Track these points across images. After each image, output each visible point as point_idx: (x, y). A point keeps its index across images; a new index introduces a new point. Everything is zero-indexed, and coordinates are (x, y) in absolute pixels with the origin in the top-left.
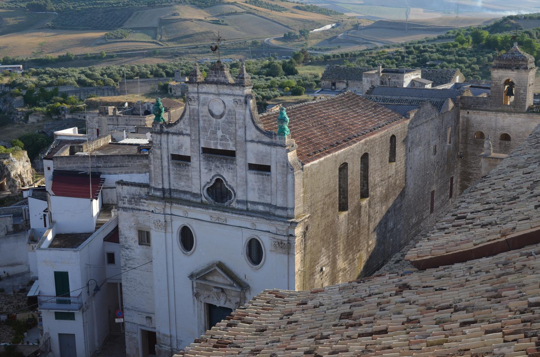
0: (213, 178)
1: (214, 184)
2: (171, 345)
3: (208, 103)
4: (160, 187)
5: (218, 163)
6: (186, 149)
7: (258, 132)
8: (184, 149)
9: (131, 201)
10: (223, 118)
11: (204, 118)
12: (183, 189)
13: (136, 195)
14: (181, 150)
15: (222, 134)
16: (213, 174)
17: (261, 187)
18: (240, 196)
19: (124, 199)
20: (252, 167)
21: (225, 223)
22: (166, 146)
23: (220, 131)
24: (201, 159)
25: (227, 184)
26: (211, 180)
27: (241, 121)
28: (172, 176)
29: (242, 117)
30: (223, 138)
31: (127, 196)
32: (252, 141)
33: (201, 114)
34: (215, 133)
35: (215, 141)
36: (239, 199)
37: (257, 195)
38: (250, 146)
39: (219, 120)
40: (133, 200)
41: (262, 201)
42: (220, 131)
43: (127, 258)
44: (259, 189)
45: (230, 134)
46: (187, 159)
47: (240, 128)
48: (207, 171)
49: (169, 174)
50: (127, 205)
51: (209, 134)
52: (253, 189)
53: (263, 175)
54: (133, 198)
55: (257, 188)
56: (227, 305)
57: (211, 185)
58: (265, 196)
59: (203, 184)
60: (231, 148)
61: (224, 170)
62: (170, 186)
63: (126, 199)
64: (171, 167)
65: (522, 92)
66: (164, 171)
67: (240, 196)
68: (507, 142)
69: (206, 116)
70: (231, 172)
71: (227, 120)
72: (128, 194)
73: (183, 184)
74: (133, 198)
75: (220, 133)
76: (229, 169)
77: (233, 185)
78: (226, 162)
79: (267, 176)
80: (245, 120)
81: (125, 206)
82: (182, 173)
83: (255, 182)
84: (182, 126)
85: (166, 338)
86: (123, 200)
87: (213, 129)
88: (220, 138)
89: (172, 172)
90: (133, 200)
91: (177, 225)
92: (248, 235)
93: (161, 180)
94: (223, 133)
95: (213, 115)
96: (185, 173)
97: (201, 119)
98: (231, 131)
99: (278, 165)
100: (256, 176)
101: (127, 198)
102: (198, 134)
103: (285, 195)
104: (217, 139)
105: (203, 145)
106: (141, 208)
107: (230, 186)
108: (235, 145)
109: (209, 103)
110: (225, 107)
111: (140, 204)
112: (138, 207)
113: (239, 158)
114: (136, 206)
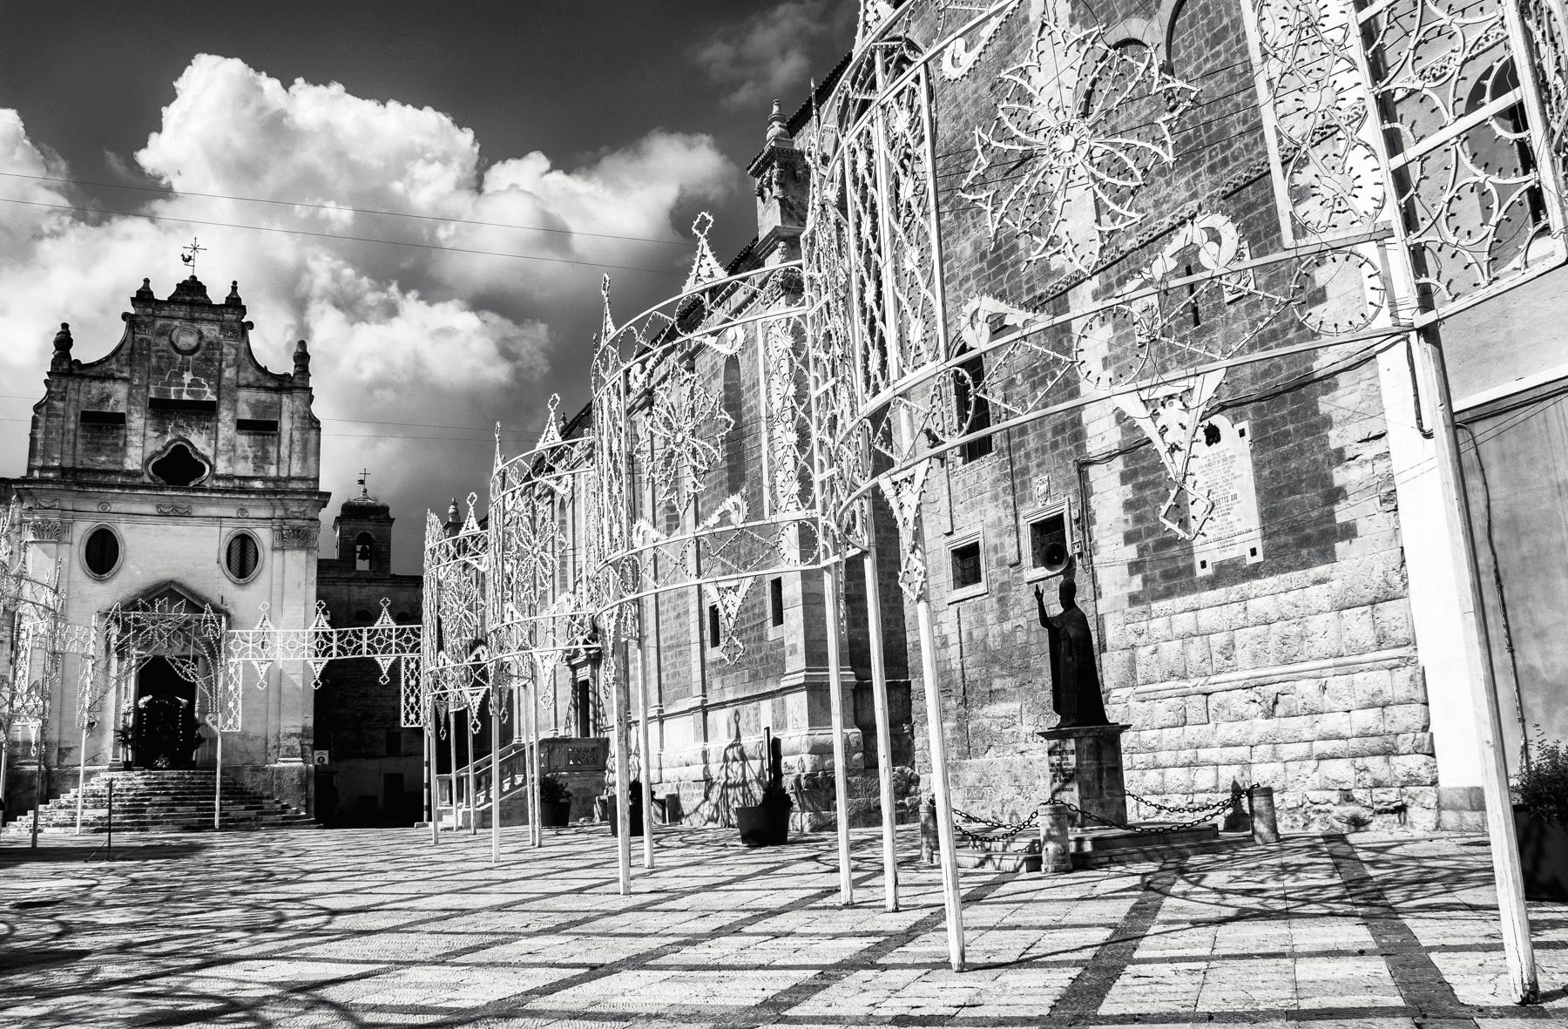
0: (170, 443)
4: (56, 464)
5: (181, 422)
8: (112, 401)
10: (197, 355)
12: (103, 467)
17: (259, 453)
18: (222, 467)
20: (242, 425)
25: (197, 453)
26: (165, 448)
28: (80, 447)
30: (194, 383)
32: (248, 386)
33: (154, 349)
34: (180, 375)
38: (243, 394)
41: (261, 474)
44: (256, 457)
45: (208, 377)
47: (228, 366)
48: (157, 434)
49: (75, 443)
52: (245, 458)
55: (251, 455)
57: (165, 455)
59: (147, 455)
60: (209, 396)
64: (79, 433)
65: (384, 549)
67: (222, 467)
73: (103, 459)
77: (209, 452)
82: (104, 441)
84: (114, 367)
89: (80, 441)
91: (82, 530)
92: (229, 530)
95: (178, 350)
96: (110, 441)
104: (183, 385)
108: (218, 393)
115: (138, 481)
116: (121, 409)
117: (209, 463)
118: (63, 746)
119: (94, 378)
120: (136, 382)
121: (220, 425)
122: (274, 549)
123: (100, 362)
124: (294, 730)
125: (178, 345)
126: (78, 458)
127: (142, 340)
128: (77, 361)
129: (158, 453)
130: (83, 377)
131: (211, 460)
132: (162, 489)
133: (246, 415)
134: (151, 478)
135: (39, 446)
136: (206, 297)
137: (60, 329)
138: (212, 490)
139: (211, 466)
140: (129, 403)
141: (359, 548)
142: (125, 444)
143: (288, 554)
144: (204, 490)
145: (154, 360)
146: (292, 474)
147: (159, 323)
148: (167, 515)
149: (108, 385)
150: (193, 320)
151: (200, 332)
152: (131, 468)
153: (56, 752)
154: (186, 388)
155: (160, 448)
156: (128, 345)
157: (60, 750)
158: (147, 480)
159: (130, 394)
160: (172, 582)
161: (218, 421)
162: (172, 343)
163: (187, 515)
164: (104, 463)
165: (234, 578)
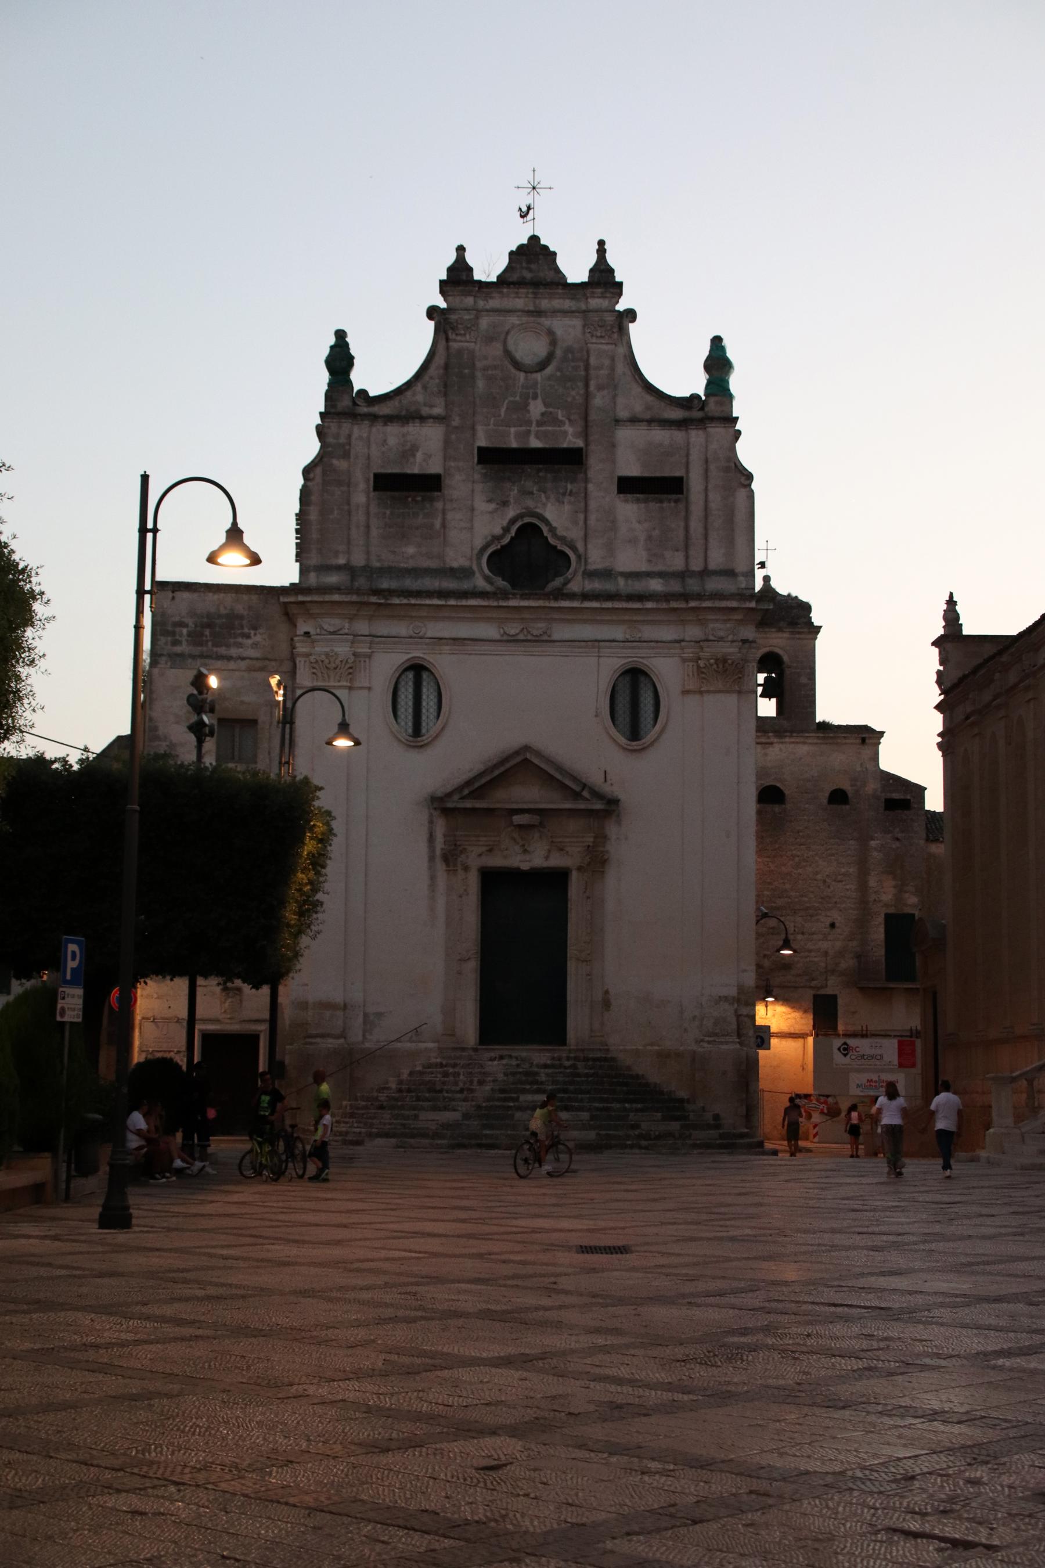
0: (513, 522)
2: (343, 1035)
3: (502, 336)
4: (342, 561)
5: (529, 485)
6: (428, 456)
7: (649, 398)
8: (419, 455)
9: (202, 635)
10: (549, 370)
11: (490, 372)
12: (410, 564)
13: (220, 616)
14: (411, 460)
15: (544, 410)
16: (511, 513)
17: (657, 532)
18: (596, 559)
19: (177, 630)
20: (627, 486)
21: (545, 638)
23: (539, 401)
24: (477, 476)
25: (555, 535)
26: (506, 530)
27: (604, 372)
28: (374, 532)
29: (607, 362)
30: (547, 419)
31: (186, 620)
32: (634, 420)
33: (479, 364)
34: (523, 407)
35: (523, 428)
36: (592, 567)
37: (644, 554)
38: (625, 435)
39: (538, 376)
40: (207, 632)
41: (660, 568)
42: (539, 401)
44: (649, 538)
46: (431, 484)
47: (600, 388)
48: (492, 506)
50: (183, 648)
51: (503, 410)
52: (633, 541)
53: (661, 502)
54: (209, 625)
55: (642, 537)
56: (556, 861)
57: (506, 540)
58: (668, 554)
59: (479, 543)
60: (571, 439)
61: (547, 498)
62: (368, 559)
63: (185, 631)
64: (374, 509)
65: (804, 680)
67: (596, 559)
68: (777, 808)
69: (495, 367)
70: (569, 502)
71: (558, 374)
72: (192, 613)
73: (411, 550)
74: (209, 625)
75: (536, 408)
76: (564, 494)
77: (574, 534)
79: (673, 504)
80: (612, 368)
81: (178, 649)
83: (639, 522)
84: (420, 398)
85: (328, 1013)
86: (173, 634)
87: (518, 398)
88: (539, 417)
90: (207, 632)
92: (612, 664)
94: (546, 405)
95: (517, 365)
97: (479, 374)
98: (569, 399)
99: (712, 467)
100: (643, 505)
101: (186, 626)
103: (730, 542)
104: (529, 423)
105: (482, 442)
106: (234, 652)
107: (563, 539)
108: (585, 434)
109: (508, 333)
110: (553, 343)
111: (232, 640)
112: (222, 650)
113: (595, 465)
114: (215, 649)
115: (465, 585)
116: (434, 467)
117: (574, 549)
119: (389, 419)
120: (456, 422)
121: (590, 486)
122: (685, 692)
123: (399, 391)
124: (725, 992)
125: (518, 356)
127: (460, 351)
128: (363, 393)
129: (496, 538)
130: (374, 418)
131: (580, 546)
132: (505, 595)
133: (633, 469)
134: (487, 579)
135: (315, 536)
136: (558, 271)
137: (332, 340)
138: (585, 596)
139: (579, 557)
140: (446, 458)
141: (761, 678)
142: (444, 525)
143: (709, 699)
144: (572, 596)
145: (481, 384)
146: (712, 566)
147: (484, 322)
148: (513, 640)
149: (413, 430)
150: (539, 313)
151: (550, 333)
152: (455, 565)
153: (360, 1019)
154: (534, 428)
155: (498, 531)
156: (440, 360)
157: (366, 1015)
158: (480, 583)
159: (447, 443)
160: (527, 748)
161: (586, 480)
162: (508, 353)
164: (412, 557)
165: (623, 740)
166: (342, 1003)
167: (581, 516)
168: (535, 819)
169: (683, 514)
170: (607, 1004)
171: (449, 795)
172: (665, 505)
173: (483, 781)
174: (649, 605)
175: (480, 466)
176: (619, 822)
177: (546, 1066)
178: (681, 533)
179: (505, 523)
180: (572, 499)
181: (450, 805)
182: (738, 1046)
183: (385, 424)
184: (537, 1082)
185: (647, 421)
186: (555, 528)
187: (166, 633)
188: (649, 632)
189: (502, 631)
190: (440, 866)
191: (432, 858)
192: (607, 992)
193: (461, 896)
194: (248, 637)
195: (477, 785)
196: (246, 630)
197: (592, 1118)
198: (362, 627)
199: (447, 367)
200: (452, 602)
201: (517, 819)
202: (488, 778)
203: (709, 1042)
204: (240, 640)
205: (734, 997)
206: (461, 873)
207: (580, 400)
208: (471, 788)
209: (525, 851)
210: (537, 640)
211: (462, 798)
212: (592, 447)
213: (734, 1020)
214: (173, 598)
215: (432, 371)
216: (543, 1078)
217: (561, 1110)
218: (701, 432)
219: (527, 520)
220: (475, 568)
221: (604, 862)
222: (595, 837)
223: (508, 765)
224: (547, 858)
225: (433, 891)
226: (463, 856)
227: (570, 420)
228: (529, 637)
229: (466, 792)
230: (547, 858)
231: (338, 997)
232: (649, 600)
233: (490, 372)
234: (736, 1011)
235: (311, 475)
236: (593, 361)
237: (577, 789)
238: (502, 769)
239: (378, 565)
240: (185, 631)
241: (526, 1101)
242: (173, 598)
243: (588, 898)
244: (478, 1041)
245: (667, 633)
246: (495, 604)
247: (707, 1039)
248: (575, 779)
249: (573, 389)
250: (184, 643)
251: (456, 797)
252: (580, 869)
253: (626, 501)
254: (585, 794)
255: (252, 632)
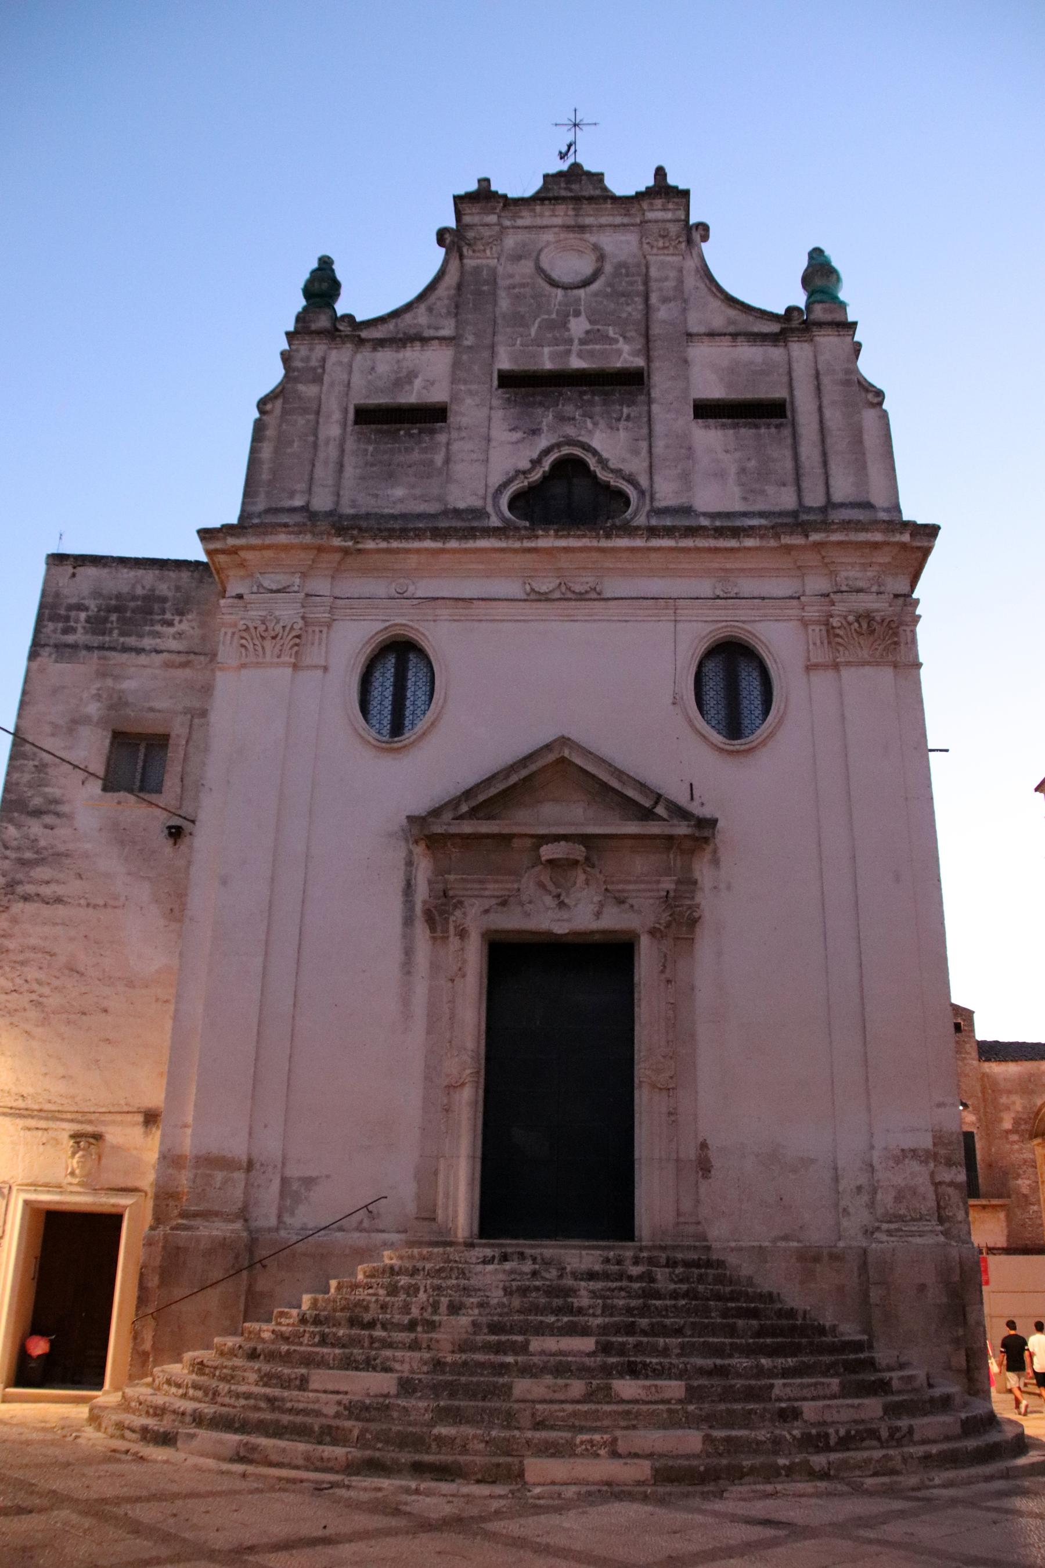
0: (547, 452)
1: (546, 478)
2: (243, 1214)
3: (534, 254)
4: (298, 502)
5: (569, 409)
6: (430, 383)
7: (732, 313)
8: (418, 383)
9: (106, 620)
10: (595, 287)
11: (517, 290)
13: (134, 598)
15: (588, 327)
16: (544, 442)
17: (753, 464)
18: (667, 493)
19: (73, 614)
21: (593, 595)
22: (345, 377)
23: (583, 318)
26: (536, 463)
27: (670, 284)
28: (349, 471)
29: (673, 274)
31: (86, 602)
33: (502, 283)
35: (561, 348)
36: (660, 504)
37: (737, 491)
38: (701, 353)
39: (581, 292)
40: (114, 617)
42: (583, 318)
43: (28, 855)
44: (743, 470)
47: (665, 300)
48: (518, 435)
49: (341, 466)
50: (79, 637)
52: (720, 475)
54: (117, 609)
55: (733, 470)
57: (536, 476)
58: (771, 490)
59: (496, 479)
61: (595, 424)
62: (337, 503)
63: (83, 615)
64: (350, 445)
66: (321, 455)
69: (523, 285)
70: (626, 429)
71: (609, 290)
72: (96, 594)
73: (399, 492)
74: (117, 609)
75: (578, 326)
76: (619, 420)
77: (636, 466)
78: (605, 403)
79: (773, 430)
80: (680, 281)
81: (70, 639)
82: (401, 458)
83: (727, 451)
85: (219, 1176)
86: (67, 619)
87: (554, 316)
88: (582, 336)
89: (349, 462)
90: (114, 617)
93: (306, 477)
94: (590, 322)
95: (554, 284)
96: (416, 456)
97: (502, 293)
98: (624, 315)
99: (826, 380)
100: (731, 431)
101: (87, 609)
102: (489, 330)
103: (860, 466)
104: (570, 341)
105: (505, 363)
107: (617, 472)
109: (541, 250)
110: (601, 258)
111: (147, 628)
112: (132, 641)
113: (661, 382)
114: (122, 639)
116: (438, 395)
117: (635, 484)
118: (294, 1171)
119: (380, 344)
120: (469, 341)
121: (655, 408)
122: (810, 668)
123: (395, 314)
124: (908, 1142)
126: (346, 495)
127: (477, 270)
128: (349, 318)
129: (520, 473)
130: (361, 342)
131: (644, 482)
133: (715, 391)
135: (265, 476)
136: (605, 189)
138: (653, 532)
139: (642, 493)
142: (447, 461)
143: (848, 674)
147: (510, 241)
148: (543, 598)
149: (412, 355)
150: (582, 228)
151: (596, 247)
152: (461, 505)
153: (275, 1186)
154: (576, 347)
155: (525, 465)
156: (451, 279)
157: (285, 1181)
159: (456, 364)
160: (564, 741)
161: (649, 402)
162: (540, 270)
163: (592, 596)
164: (401, 501)
165: (718, 739)
166: (244, 1158)
167: (644, 445)
168: (578, 851)
169: (789, 441)
170: (704, 1167)
171: (436, 812)
172: (763, 430)
173: (493, 791)
174: (749, 542)
175: (500, 391)
176: (716, 862)
177: (591, 1276)
178: (789, 464)
179: (535, 455)
180: (630, 424)
181: (438, 829)
182: (942, 1239)
183: (374, 349)
184: (570, 1310)
185: (731, 334)
186: (607, 460)
187: (55, 618)
188: (748, 586)
189: (528, 588)
190: (421, 931)
191: (408, 921)
192: (704, 1146)
193: (452, 981)
194: (170, 624)
195: (481, 798)
196: (168, 616)
197: (693, 1394)
198: (321, 585)
199: (459, 287)
200: (453, 544)
201: (547, 852)
202: (501, 786)
203: (889, 1233)
204: (158, 628)
205: (927, 1151)
206: (454, 942)
207: (638, 316)
208: (473, 803)
209: (562, 905)
210: (581, 597)
211: (461, 817)
212: (656, 364)
213: (931, 1195)
214: (74, 575)
215: (441, 291)
216: (584, 1301)
217: (621, 1376)
218: (806, 345)
219: (566, 450)
220: (490, 509)
221: (693, 922)
222: (679, 882)
223: (533, 767)
224: (598, 915)
225: (409, 973)
226: (458, 913)
227: (625, 338)
228: (569, 595)
229: (464, 808)
230: (598, 915)
231: (237, 1148)
232: (749, 536)
233: (517, 290)
234: (932, 1174)
235: (269, 407)
236: (653, 272)
237: (647, 803)
238: (524, 773)
239: (351, 511)
240: (83, 615)
241: (543, 1353)
242: (74, 575)
243: (669, 981)
244: (476, 1229)
245: (780, 587)
246: (517, 545)
247: (885, 1226)
248: (643, 787)
249: (628, 304)
250: (80, 630)
251: (447, 816)
252: (653, 932)
253: (707, 427)
254: (660, 810)
255: (177, 618)
